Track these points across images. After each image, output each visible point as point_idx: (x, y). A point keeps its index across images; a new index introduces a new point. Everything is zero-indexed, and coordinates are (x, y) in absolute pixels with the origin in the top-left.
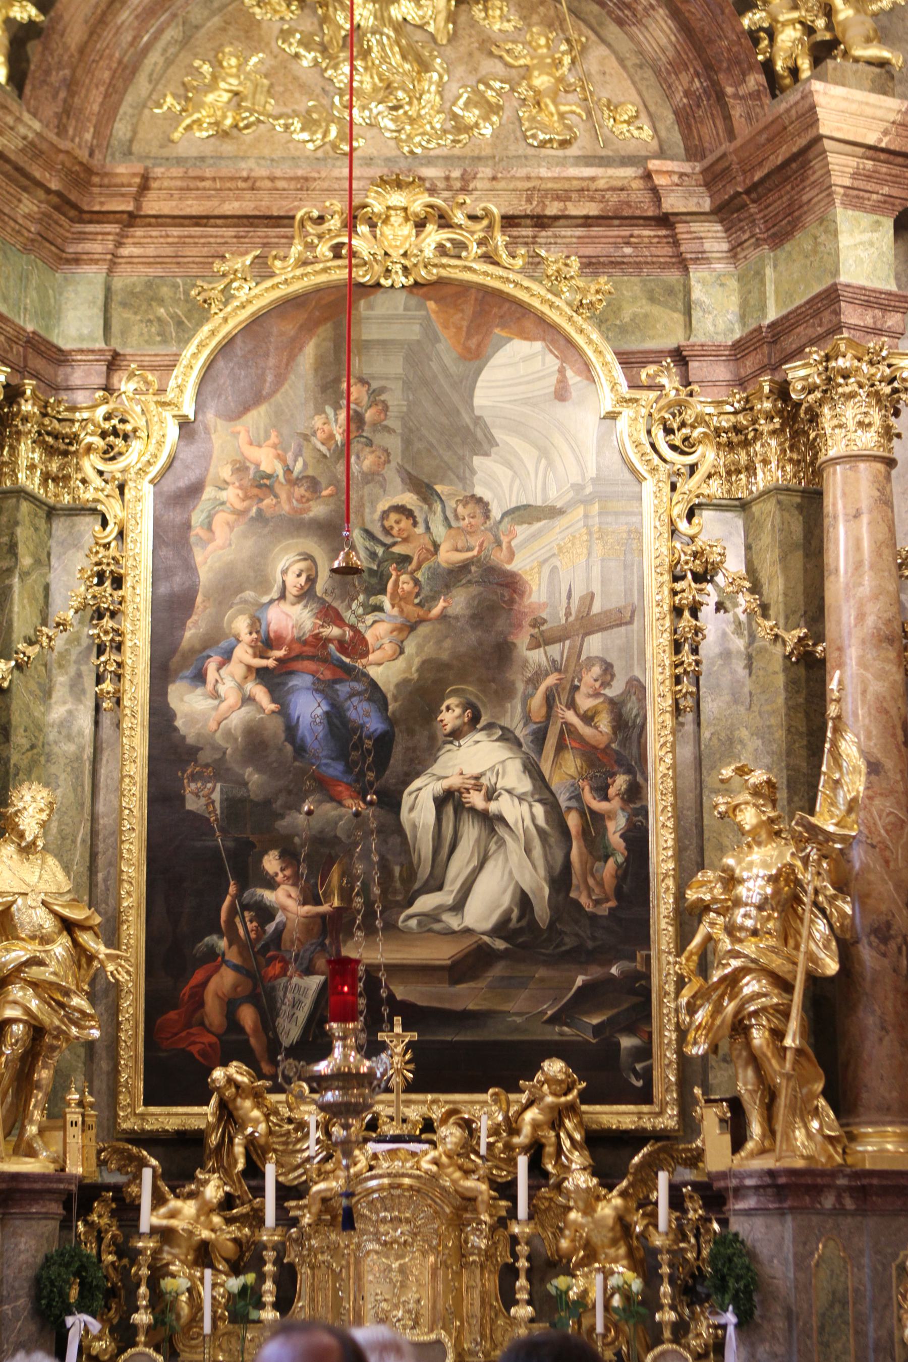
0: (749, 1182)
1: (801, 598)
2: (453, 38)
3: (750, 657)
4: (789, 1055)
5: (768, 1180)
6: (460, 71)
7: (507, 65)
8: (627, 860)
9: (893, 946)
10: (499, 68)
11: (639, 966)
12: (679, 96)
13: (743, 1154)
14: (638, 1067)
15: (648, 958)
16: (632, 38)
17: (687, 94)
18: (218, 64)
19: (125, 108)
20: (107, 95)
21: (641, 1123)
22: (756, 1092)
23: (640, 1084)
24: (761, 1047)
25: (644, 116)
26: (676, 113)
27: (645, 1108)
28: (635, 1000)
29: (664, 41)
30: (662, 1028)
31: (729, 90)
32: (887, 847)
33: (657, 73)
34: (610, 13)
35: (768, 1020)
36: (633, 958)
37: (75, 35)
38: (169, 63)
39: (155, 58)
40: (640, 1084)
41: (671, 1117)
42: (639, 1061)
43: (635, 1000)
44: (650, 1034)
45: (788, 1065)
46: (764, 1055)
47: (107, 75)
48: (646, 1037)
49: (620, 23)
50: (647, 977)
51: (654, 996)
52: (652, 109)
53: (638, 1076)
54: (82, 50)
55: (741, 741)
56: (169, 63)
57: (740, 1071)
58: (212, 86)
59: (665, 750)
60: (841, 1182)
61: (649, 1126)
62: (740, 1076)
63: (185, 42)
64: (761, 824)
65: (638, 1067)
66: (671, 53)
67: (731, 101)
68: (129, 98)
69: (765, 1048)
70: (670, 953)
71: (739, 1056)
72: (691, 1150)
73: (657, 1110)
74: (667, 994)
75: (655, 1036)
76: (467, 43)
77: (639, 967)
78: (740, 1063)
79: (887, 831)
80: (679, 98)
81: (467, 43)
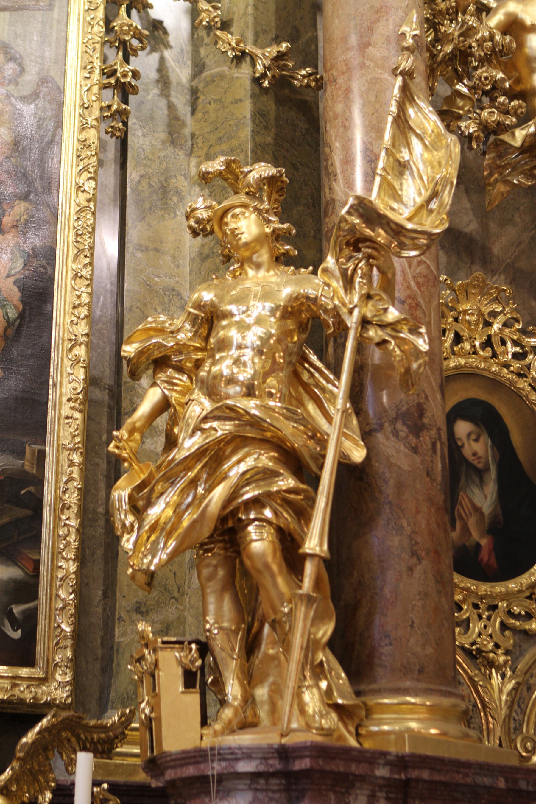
0: (244, 767)
1: (273, 18)
3: (194, 92)
4: (309, 568)
5: (276, 764)
8: (21, 316)
9: (426, 438)
11: (29, 467)
13: (218, 727)
14: (17, 609)
15: (41, 456)
21: (16, 692)
22: (236, 632)
23: (17, 635)
24: (263, 555)
27: (24, 672)
28: (21, 513)
30: (56, 554)
32: (418, 305)
35: (276, 513)
36: (21, 454)
40: (17, 635)
41: (61, 685)
42: (18, 602)
43: (21, 513)
44: (37, 564)
45: (307, 583)
46: (267, 566)
48: (31, 567)
50: (40, 482)
51: (47, 510)
53: (15, 624)
55: (178, 193)
57: (211, 599)
59: (85, 175)
60: (382, 772)
61: (28, 697)
62: (211, 608)
64: (261, 239)
65: (17, 609)
69: (270, 559)
70: (74, 449)
71: (210, 578)
72: (104, 728)
73: (41, 675)
74: (66, 507)
75: (43, 568)
77: (27, 468)
78: (212, 587)
79: (417, 283)
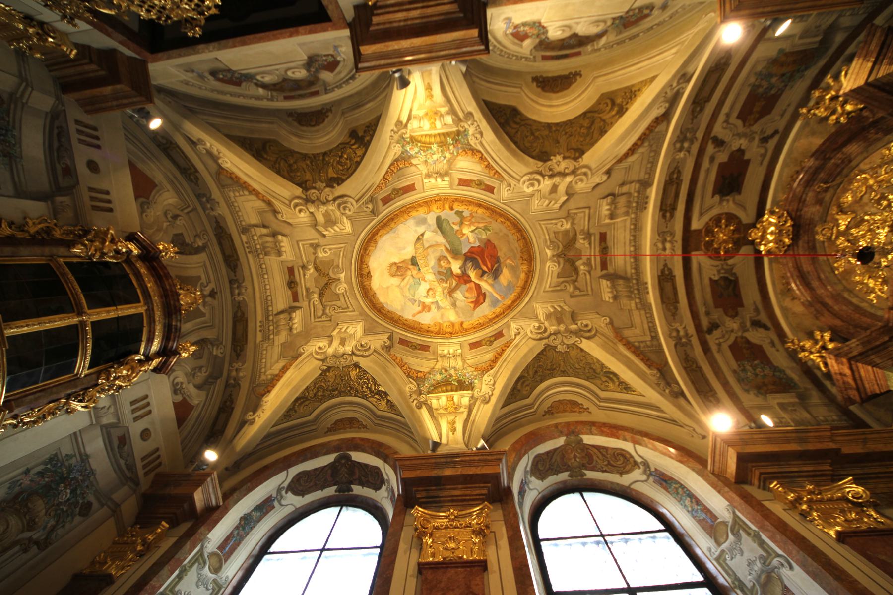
2: (853, 212)
6: (867, 208)
7: (865, 194)
10: (867, 196)
12: (878, 136)
16: (856, 157)
17: (877, 133)
18: (858, 282)
19: (872, 311)
20: (865, 316)
25: (888, 146)
26: (886, 135)
29: (856, 146)
31: (871, 120)
33: (870, 145)
34: (847, 165)
37: (838, 323)
38: (857, 296)
39: (855, 301)
47: (857, 316)
49: (850, 161)
52: (884, 144)
54: (843, 321)
56: (857, 296)
58: (867, 284)
63: (850, 291)
66: (861, 143)
67: (876, 118)
68: (869, 309)
76: (857, 207)
80: (879, 135)
81: (857, 207)
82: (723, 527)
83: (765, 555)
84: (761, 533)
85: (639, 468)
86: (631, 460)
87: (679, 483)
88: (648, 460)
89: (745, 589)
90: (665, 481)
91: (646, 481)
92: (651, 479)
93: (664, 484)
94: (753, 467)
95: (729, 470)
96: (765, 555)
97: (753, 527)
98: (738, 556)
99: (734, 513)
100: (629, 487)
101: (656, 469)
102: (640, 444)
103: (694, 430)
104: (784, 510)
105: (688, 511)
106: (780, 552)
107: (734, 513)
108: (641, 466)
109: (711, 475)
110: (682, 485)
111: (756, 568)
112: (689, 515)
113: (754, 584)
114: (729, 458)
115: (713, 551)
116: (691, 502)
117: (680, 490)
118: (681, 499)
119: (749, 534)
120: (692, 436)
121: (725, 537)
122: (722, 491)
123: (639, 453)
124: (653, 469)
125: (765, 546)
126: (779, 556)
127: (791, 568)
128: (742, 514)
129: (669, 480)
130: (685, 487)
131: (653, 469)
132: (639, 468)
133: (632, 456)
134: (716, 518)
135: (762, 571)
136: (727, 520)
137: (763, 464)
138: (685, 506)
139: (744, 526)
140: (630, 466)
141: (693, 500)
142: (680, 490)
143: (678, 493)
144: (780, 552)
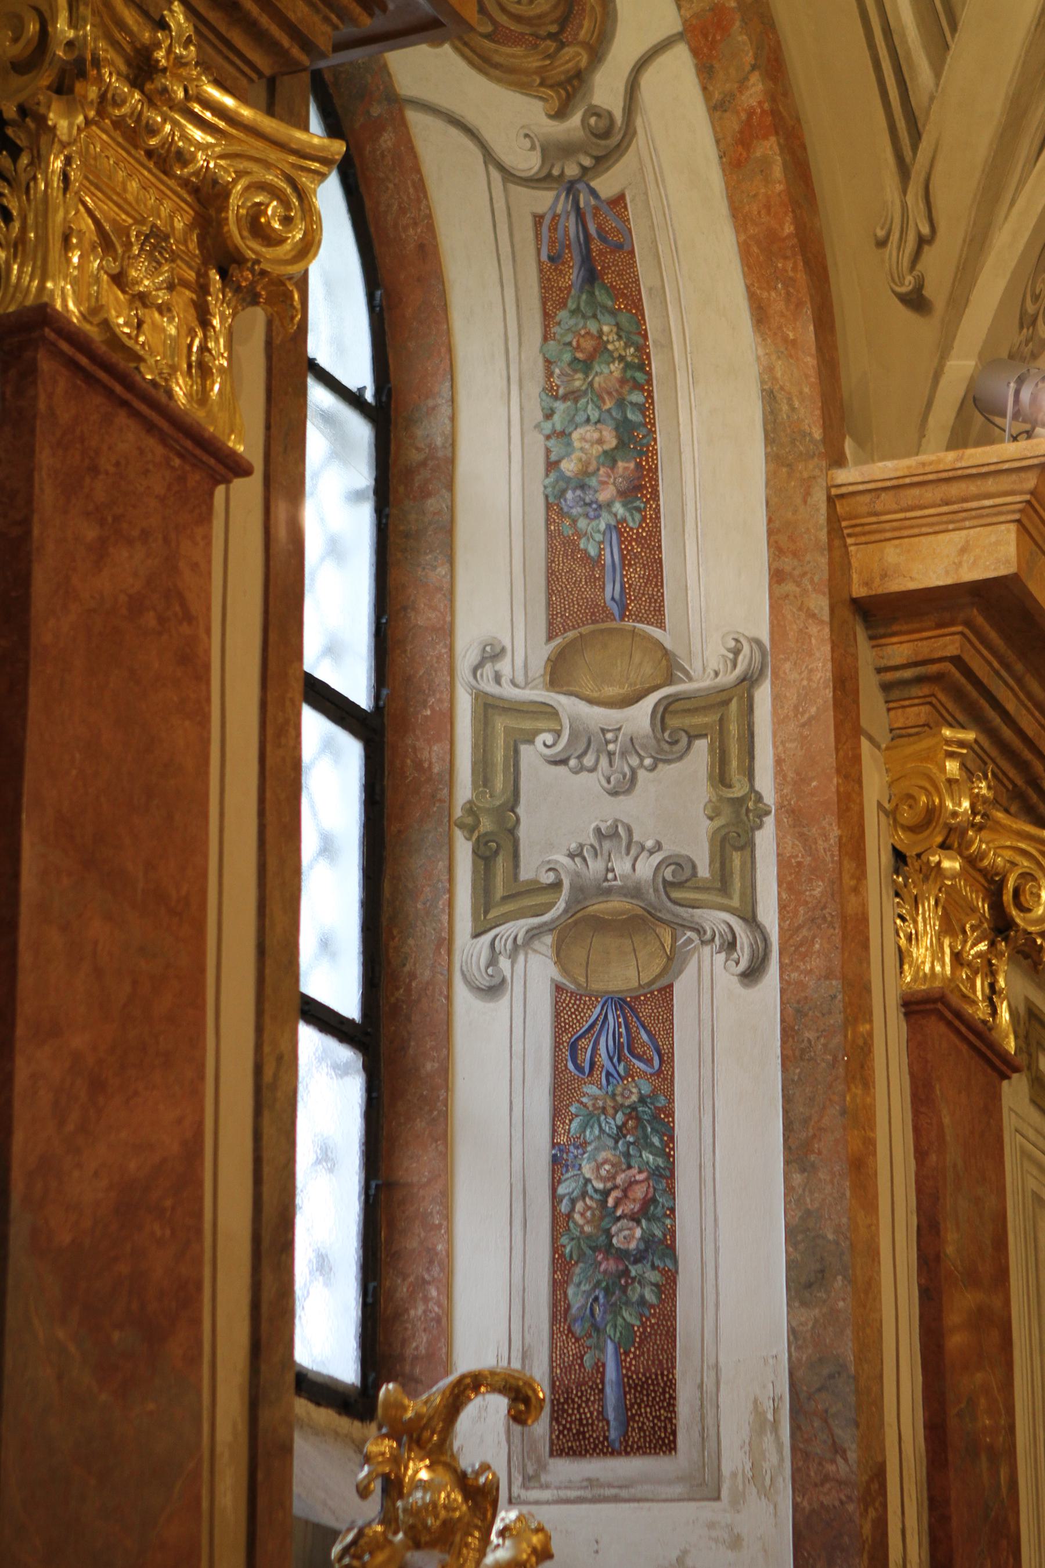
82: (647, 669)
83: (704, 871)
84: (770, 821)
85: (560, 114)
86: (573, 56)
87: (642, 350)
88: (641, 138)
89: (501, 864)
90: (591, 277)
91: (508, 175)
92: (544, 200)
93: (573, 275)
94: (968, 623)
95: (891, 554)
96: (704, 871)
97: (765, 783)
98: (592, 782)
99: (749, 681)
100: (396, 103)
101: (618, 201)
102: (706, 71)
103: (922, 242)
104: (880, 805)
105: (552, 465)
106: (769, 915)
107: (749, 681)
108: (575, 120)
109: (819, 497)
110: (643, 365)
111: (622, 866)
112: (538, 483)
113: (557, 885)
114: (958, 537)
115: (504, 666)
116: (610, 458)
117: (607, 373)
118: (573, 396)
119: (720, 777)
120: (882, 243)
121: (611, 691)
122: (789, 587)
123: (648, 79)
124: (606, 185)
125: (737, 859)
126: (751, 920)
127: (752, 974)
128: (779, 721)
129: (614, 292)
130: (645, 387)
131: (606, 185)
132: (560, 114)
133: (597, 51)
134: (656, 614)
135: (635, 892)
136: (695, 668)
137: (993, 635)
138: (563, 435)
139: (734, 749)
140: (534, 62)
141: (625, 466)
142: (607, 373)
143: (586, 365)
144: (769, 915)
